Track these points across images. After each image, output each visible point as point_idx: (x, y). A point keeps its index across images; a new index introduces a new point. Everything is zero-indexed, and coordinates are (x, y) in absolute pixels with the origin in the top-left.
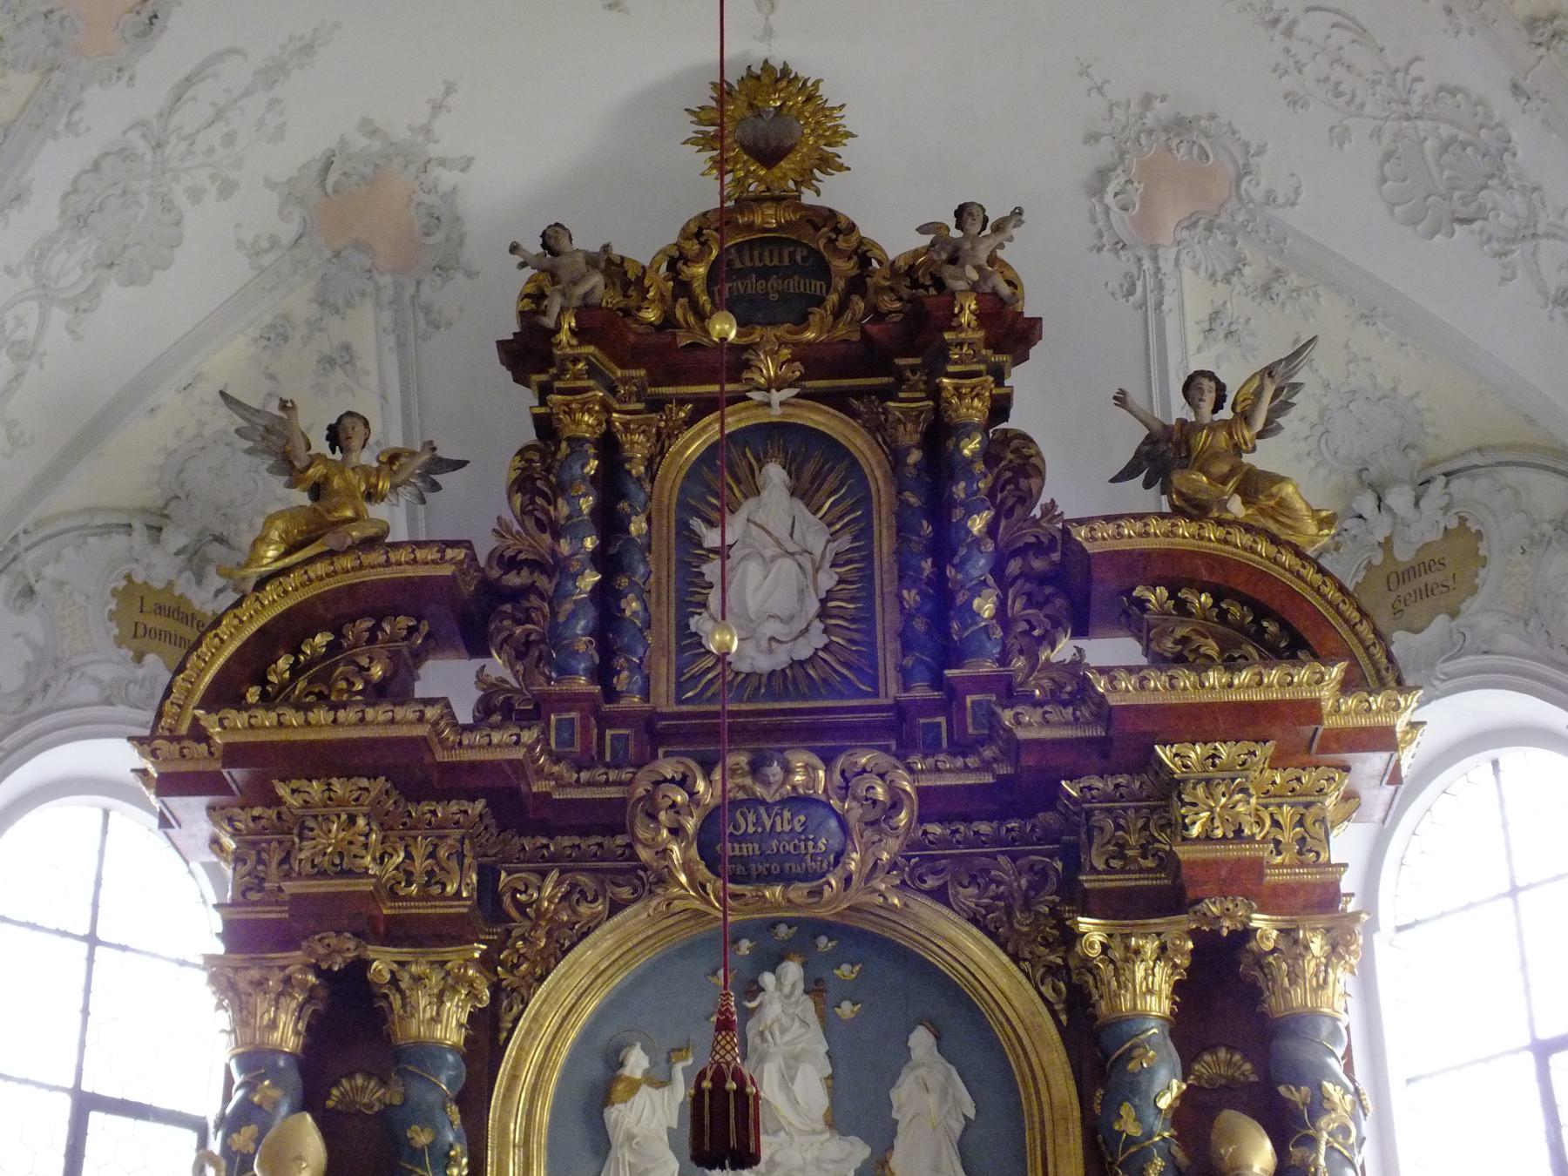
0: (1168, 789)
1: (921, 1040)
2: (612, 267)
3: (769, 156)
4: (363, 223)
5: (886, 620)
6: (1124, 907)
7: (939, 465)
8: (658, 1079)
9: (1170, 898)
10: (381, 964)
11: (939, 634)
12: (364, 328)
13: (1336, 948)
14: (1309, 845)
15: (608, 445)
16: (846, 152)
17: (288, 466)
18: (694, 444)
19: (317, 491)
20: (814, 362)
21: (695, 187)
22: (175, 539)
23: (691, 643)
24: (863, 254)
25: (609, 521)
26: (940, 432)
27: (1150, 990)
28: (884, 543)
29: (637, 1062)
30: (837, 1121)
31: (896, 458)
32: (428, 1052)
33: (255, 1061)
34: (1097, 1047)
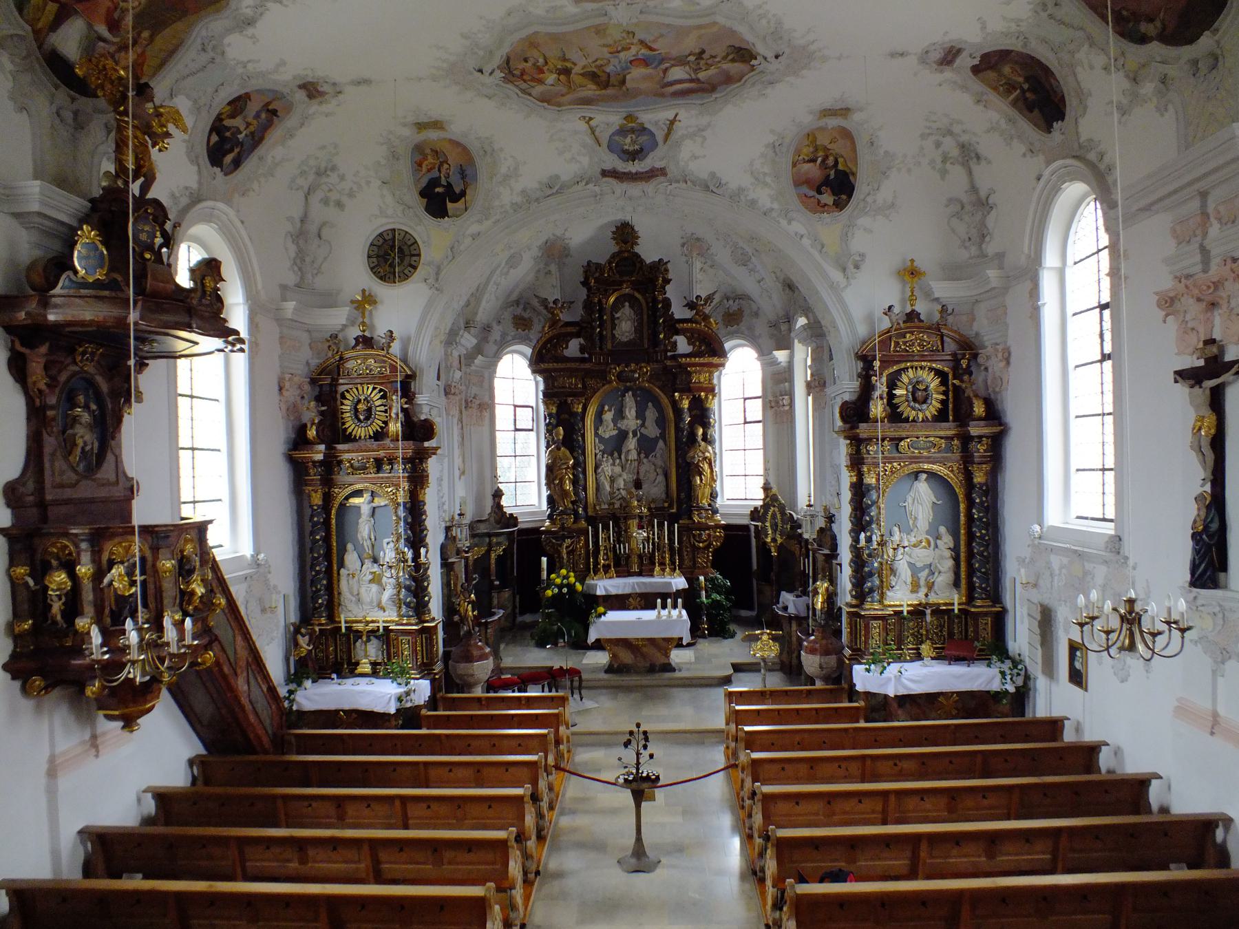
0: (689, 374)
1: (650, 404)
2: (598, 265)
3: (625, 242)
4: (554, 252)
5: (645, 335)
6: (681, 391)
7: (654, 309)
8: (610, 410)
9: (687, 389)
10: (569, 400)
11: (655, 341)
12: (553, 268)
13: (714, 396)
14: (710, 380)
15: (600, 301)
16: (639, 241)
17: (546, 308)
18: (612, 300)
19: (552, 313)
20: (632, 283)
21: (613, 248)
22: (521, 306)
23: (613, 335)
24: (642, 261)
25: (601, 318)
26: (655, 301)
27: (685, 404)
28: (645, 317)
29: (606, 408)
30: (637, 418)
31: (647, 303)
32: (575, 414)
33: (550, 415)
34: (678, 412)
